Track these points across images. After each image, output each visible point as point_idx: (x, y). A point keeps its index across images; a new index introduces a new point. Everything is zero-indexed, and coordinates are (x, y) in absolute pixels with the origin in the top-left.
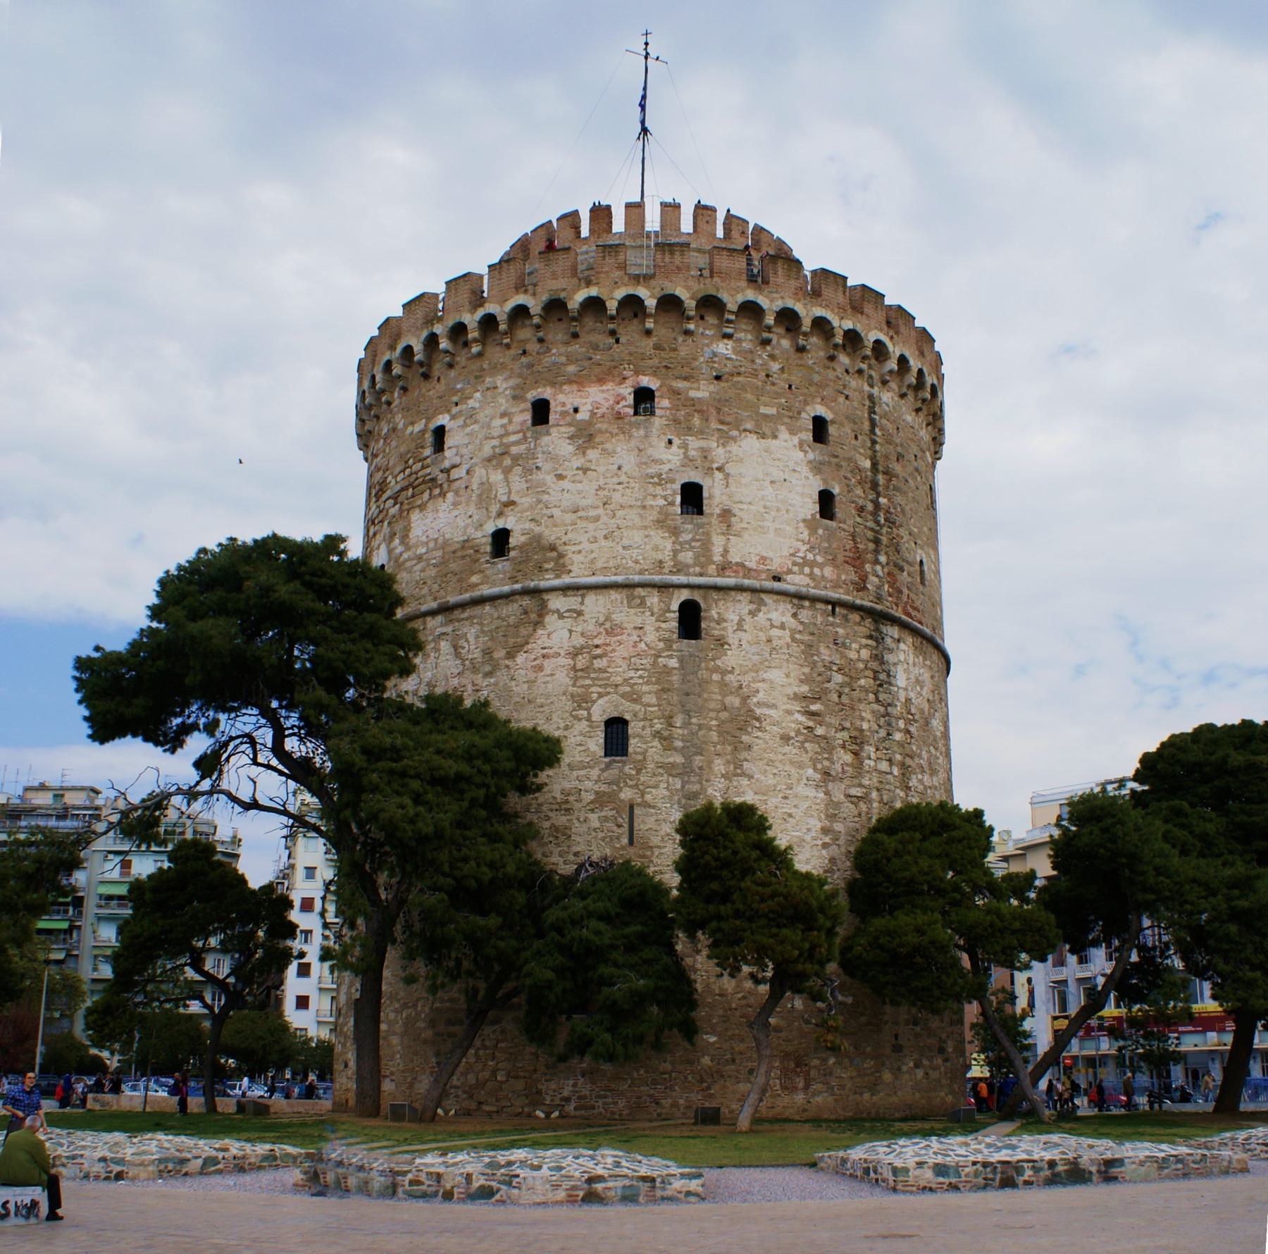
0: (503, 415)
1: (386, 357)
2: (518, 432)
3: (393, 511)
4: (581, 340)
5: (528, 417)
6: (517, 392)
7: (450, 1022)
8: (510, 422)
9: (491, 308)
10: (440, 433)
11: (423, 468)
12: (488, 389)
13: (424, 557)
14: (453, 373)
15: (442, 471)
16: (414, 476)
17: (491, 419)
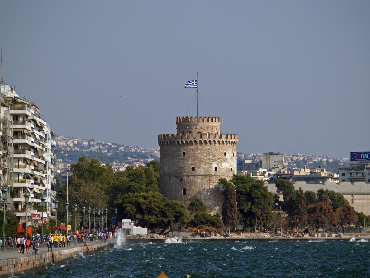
1: (219, 140)
9: (233, 141)
10: (225, 153)
14: (226, 146)
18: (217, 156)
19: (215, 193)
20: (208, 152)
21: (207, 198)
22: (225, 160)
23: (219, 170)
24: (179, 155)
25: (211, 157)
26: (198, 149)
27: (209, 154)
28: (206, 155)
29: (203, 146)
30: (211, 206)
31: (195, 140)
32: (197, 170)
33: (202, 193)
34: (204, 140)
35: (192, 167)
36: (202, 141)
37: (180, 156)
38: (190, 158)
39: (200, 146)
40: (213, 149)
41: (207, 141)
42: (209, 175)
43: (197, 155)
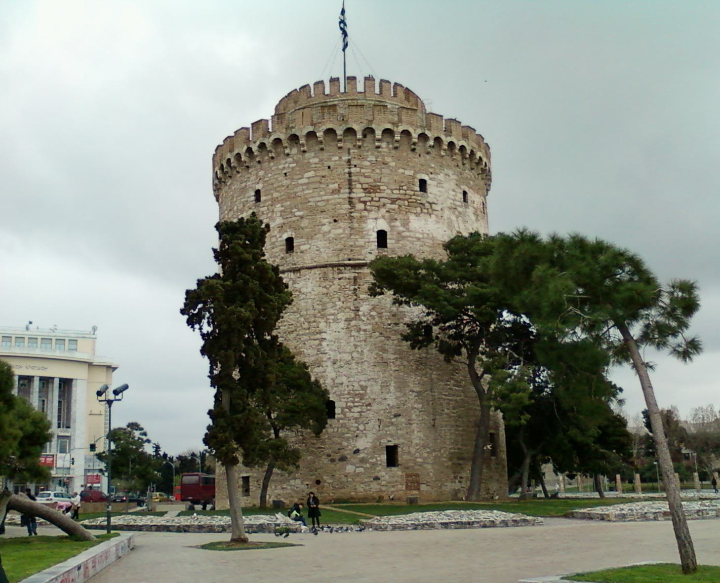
0: (453, 190)
1: (389, 126)
2: (460, 202)
3: (389, 206)
4: (473, 171)
5: (461, 196)
6: (458, 183)
7: (459, 459)
8: (456, 195)
11: (414, 195)
12: (446, 175)
13: (421, 240)
14: (428, 157)
15: (428, 202)
16: (410, 197)
17: (449, 189)
18: (381, 188)
19: (381, 334)
20: (345, 173)
21: (347, 357)
22: (427, 209)
23: (398, 241)
24: (244, 206)
25: (358, 193)
26: (306, 167)
27: (350, 182)
28: (336, 185)
29: (325, 155)
30: (364, 388)
31: (294, 131)
32: (303, 248)
33: (324, 335)
34: (324, 128)
35: (285, 236)
36: (318, 134)
37: (246, 209)
38: (278, 207)
39: (313, 154)
40: (368, 163)
41: (340, 132)
42: (351, 262)
43: (303, 190)
